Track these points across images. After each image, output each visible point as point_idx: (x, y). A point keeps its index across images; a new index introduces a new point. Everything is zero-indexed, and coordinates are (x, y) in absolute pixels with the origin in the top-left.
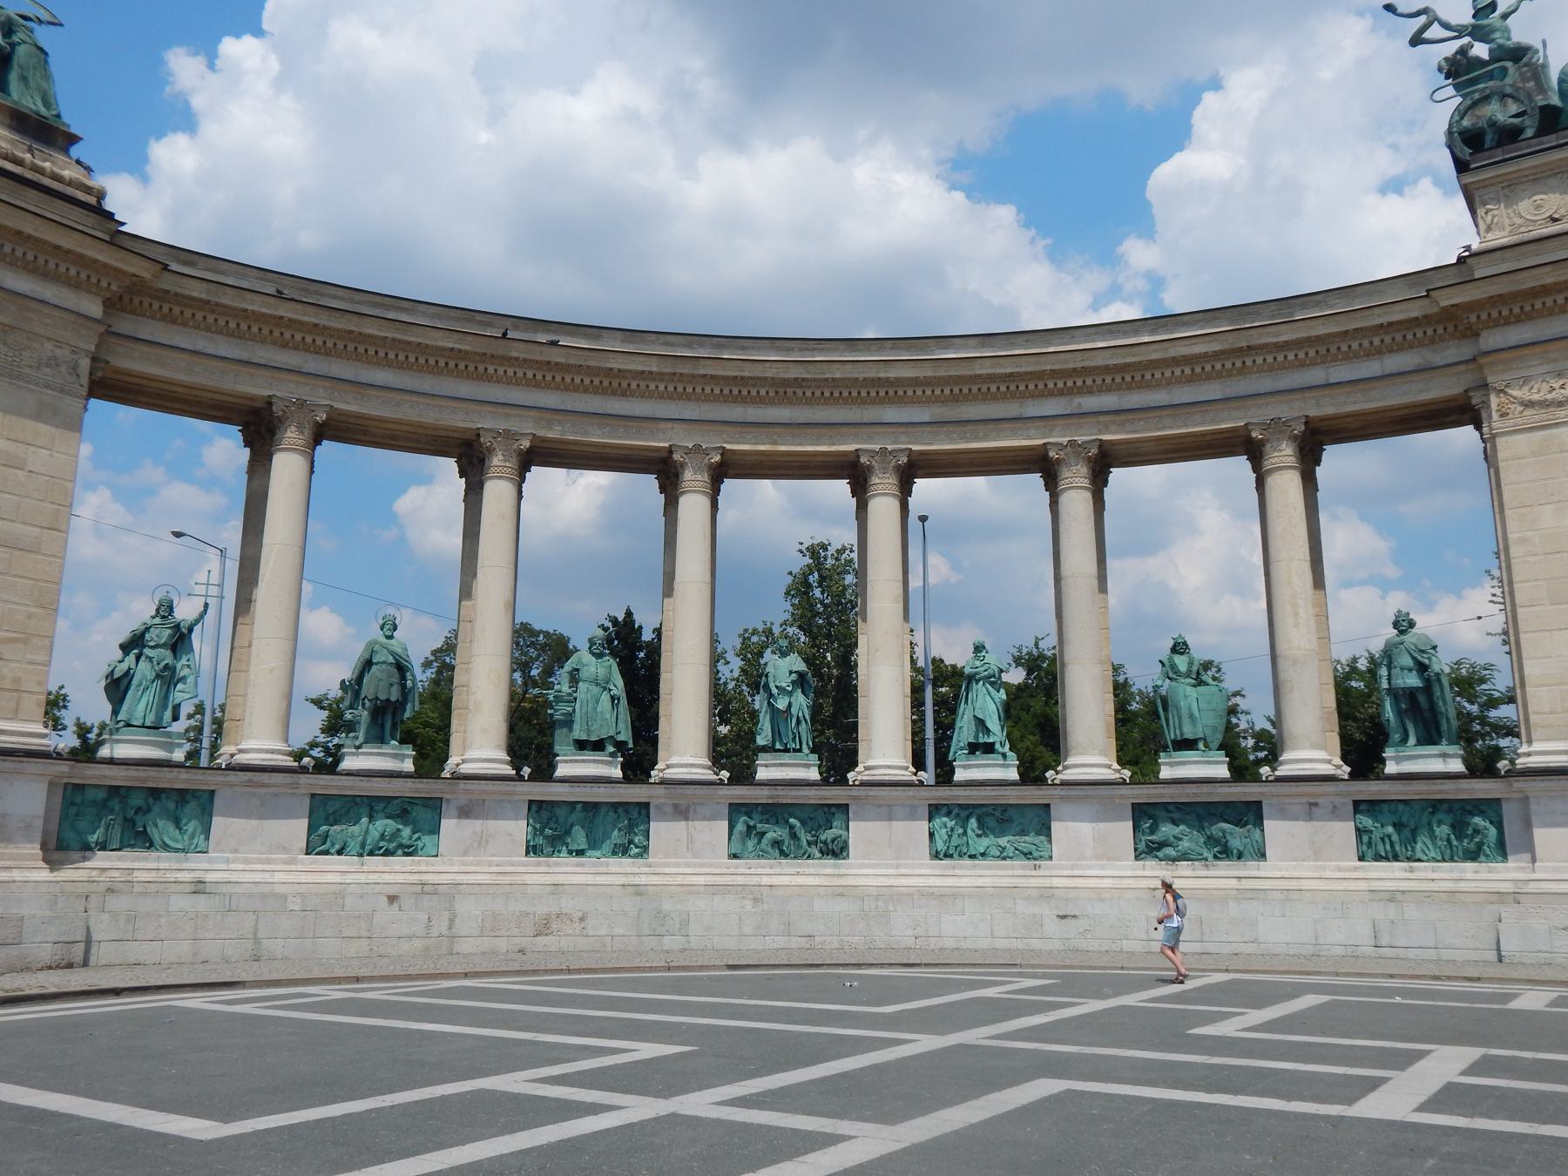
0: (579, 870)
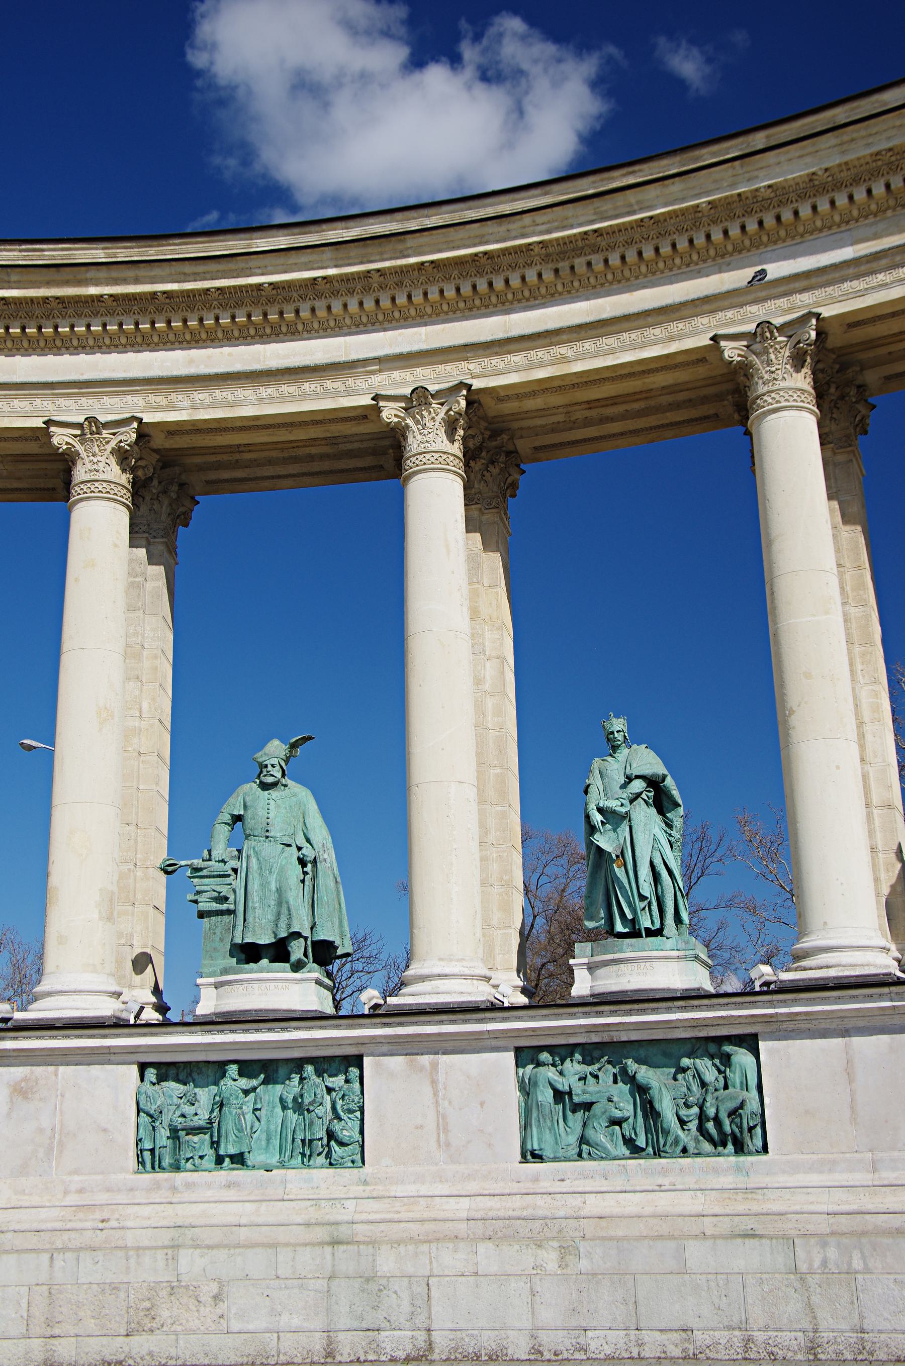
0: (231, 1194)
